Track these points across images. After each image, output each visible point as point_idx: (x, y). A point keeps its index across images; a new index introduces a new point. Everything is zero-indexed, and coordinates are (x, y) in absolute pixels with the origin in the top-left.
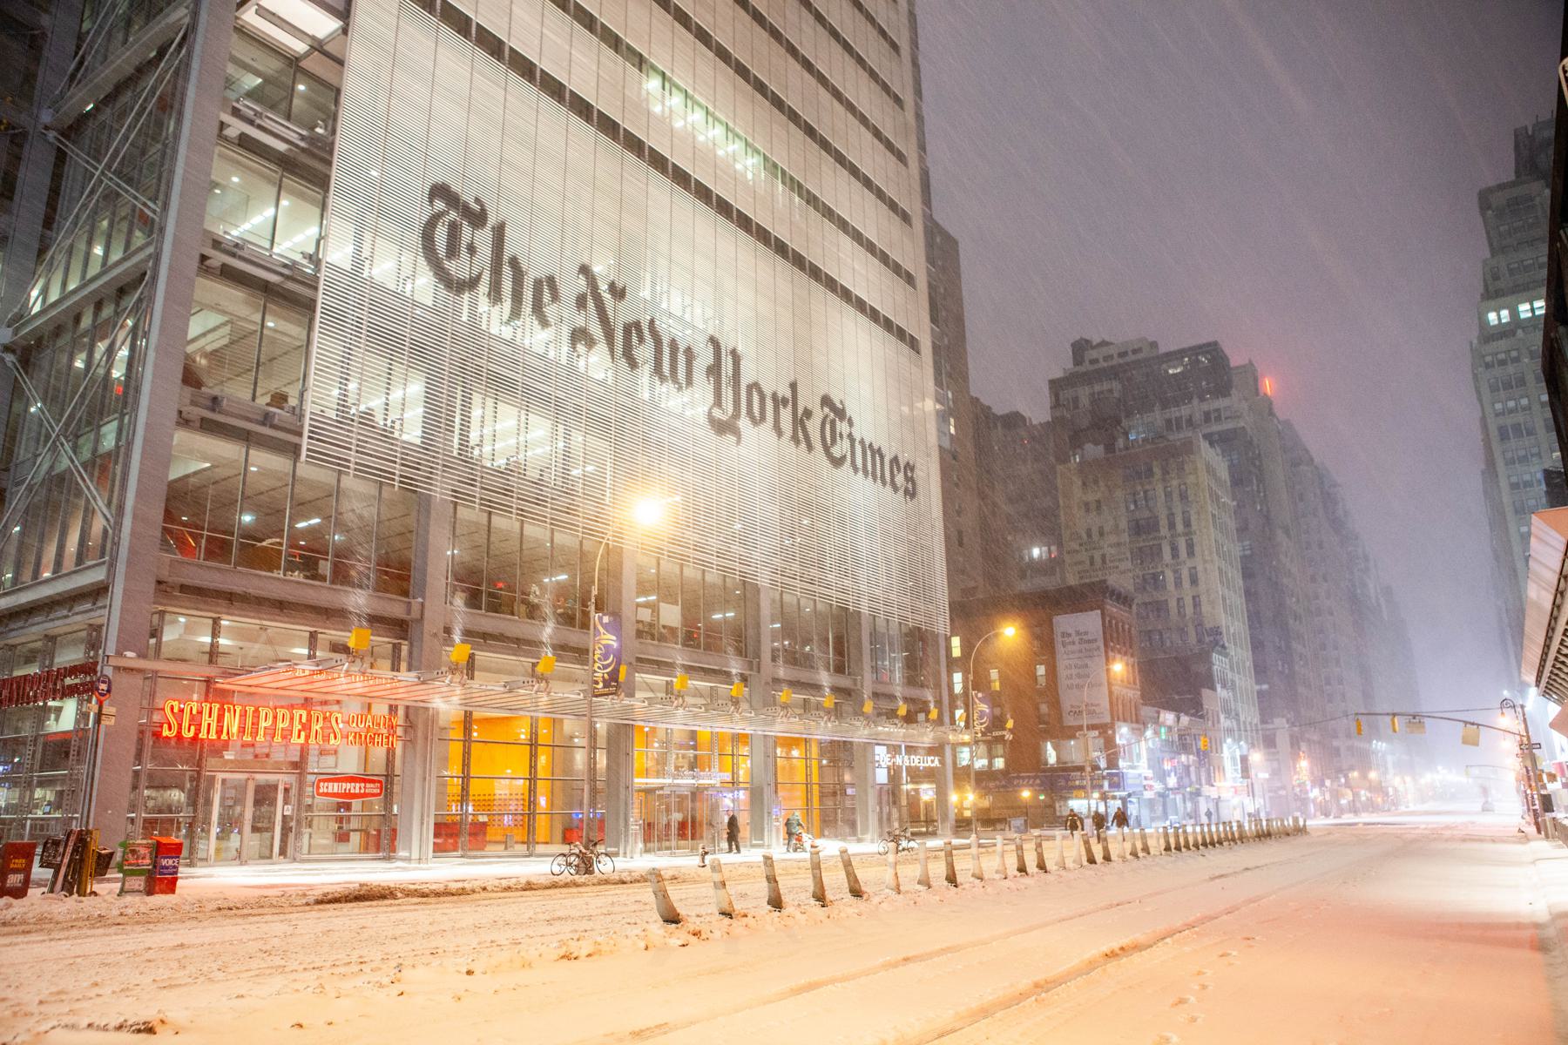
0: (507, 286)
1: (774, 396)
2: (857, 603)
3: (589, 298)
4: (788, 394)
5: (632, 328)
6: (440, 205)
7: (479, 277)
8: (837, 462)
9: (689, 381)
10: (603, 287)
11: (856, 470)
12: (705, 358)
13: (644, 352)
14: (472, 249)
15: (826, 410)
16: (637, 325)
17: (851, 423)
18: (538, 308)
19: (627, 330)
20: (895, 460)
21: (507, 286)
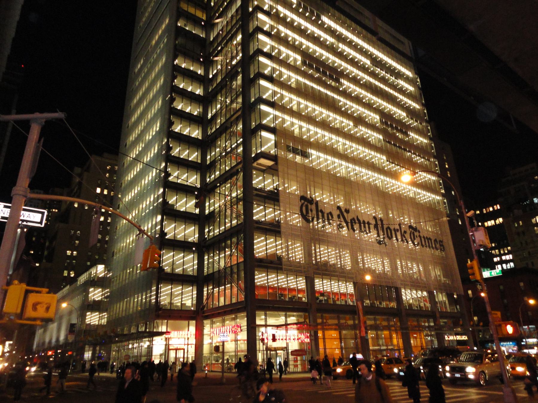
1: (394, 229)
4: (398, 228)
5: (353, 221)
6: (303, 201)
9: (370, 232)
10: (343, 210)
11: (423, 246)
12: (373, 222)
13: (356, 227)
17: (419, 232)
18: (328, 220)
20: (435, 240)
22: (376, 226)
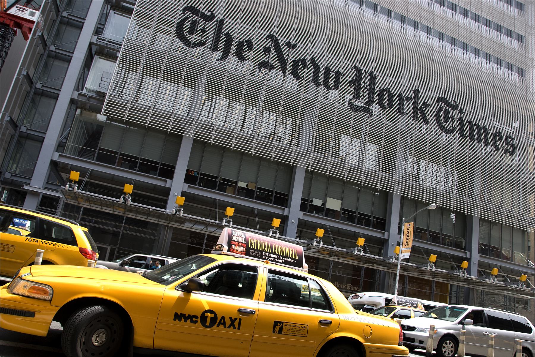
0: (221, 45)
1: (400, 96)
2: (471, 210)
3: (273, 48)
4: (412, 95)
7: (206, 41)
8: (448, 132)
14: (203, 30)
15: (442, 104)
16: (304, 61)
17: (461, 112)
19: (296, 63)
21: (221, 45)
22: (356, 83)
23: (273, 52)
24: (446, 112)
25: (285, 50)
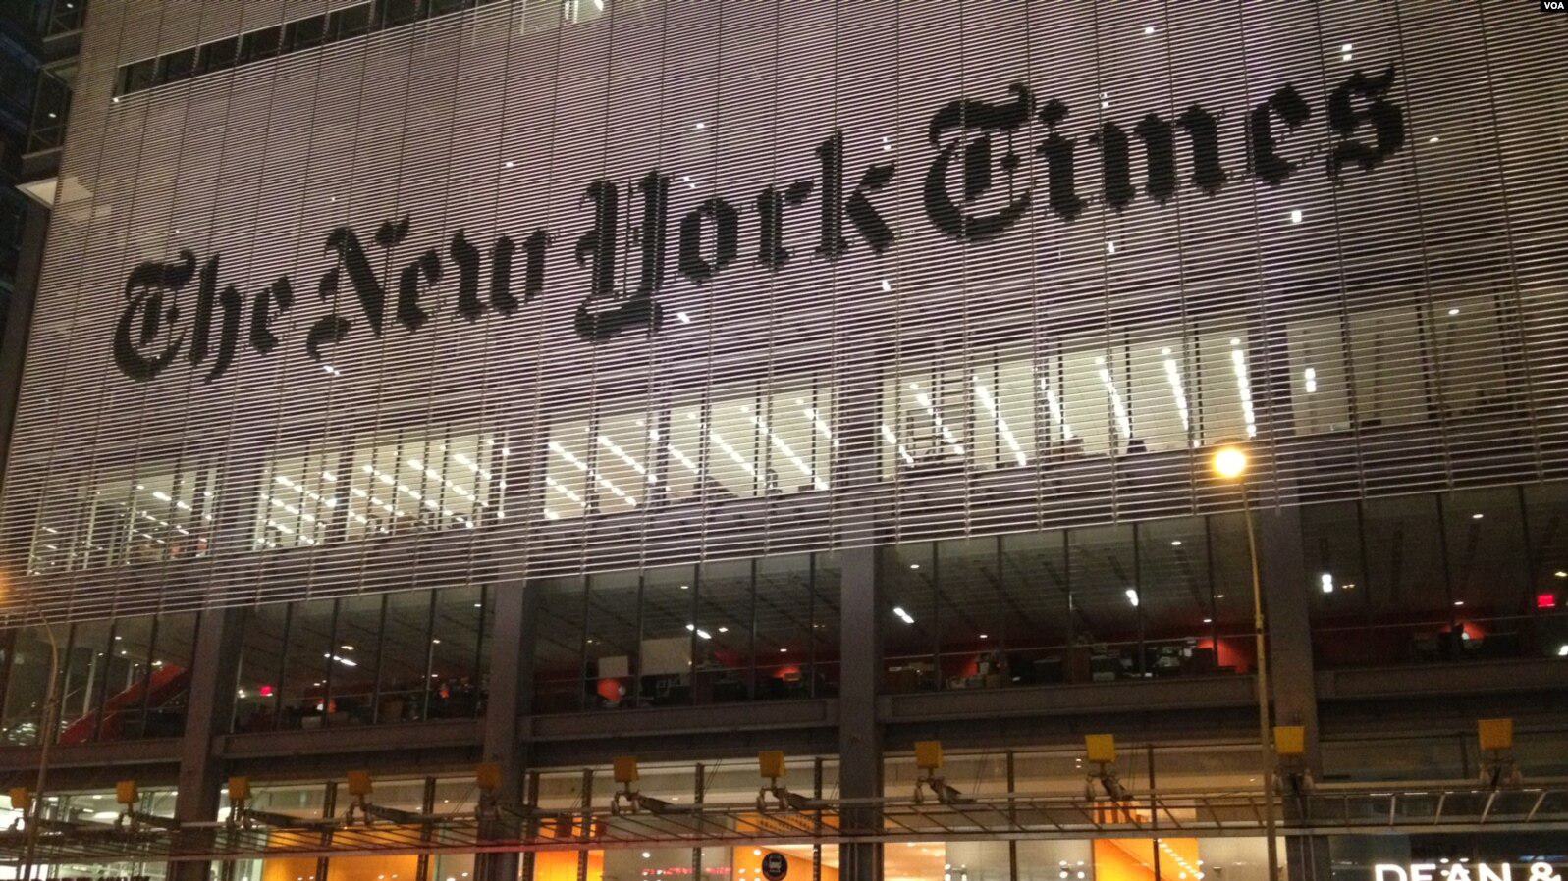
4: (813, 169)
19: (409, 278)
23: (345, 281)
24: (978, 157)
25: (375, 255)
